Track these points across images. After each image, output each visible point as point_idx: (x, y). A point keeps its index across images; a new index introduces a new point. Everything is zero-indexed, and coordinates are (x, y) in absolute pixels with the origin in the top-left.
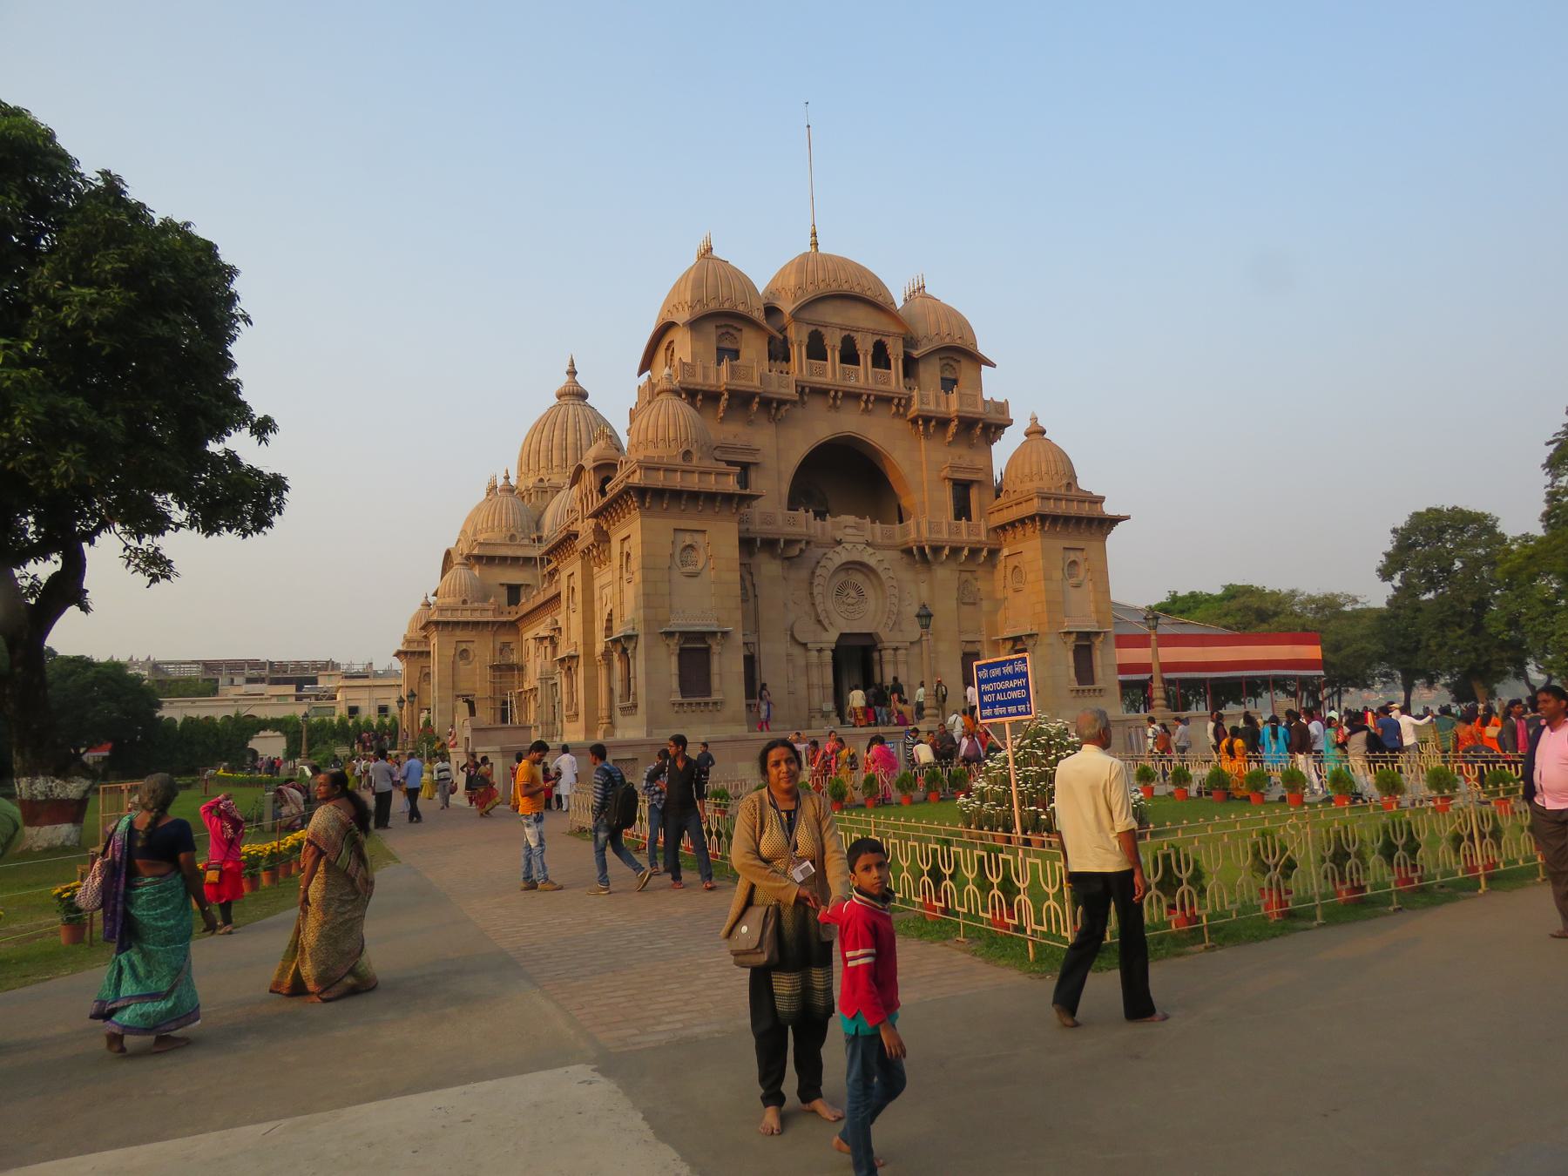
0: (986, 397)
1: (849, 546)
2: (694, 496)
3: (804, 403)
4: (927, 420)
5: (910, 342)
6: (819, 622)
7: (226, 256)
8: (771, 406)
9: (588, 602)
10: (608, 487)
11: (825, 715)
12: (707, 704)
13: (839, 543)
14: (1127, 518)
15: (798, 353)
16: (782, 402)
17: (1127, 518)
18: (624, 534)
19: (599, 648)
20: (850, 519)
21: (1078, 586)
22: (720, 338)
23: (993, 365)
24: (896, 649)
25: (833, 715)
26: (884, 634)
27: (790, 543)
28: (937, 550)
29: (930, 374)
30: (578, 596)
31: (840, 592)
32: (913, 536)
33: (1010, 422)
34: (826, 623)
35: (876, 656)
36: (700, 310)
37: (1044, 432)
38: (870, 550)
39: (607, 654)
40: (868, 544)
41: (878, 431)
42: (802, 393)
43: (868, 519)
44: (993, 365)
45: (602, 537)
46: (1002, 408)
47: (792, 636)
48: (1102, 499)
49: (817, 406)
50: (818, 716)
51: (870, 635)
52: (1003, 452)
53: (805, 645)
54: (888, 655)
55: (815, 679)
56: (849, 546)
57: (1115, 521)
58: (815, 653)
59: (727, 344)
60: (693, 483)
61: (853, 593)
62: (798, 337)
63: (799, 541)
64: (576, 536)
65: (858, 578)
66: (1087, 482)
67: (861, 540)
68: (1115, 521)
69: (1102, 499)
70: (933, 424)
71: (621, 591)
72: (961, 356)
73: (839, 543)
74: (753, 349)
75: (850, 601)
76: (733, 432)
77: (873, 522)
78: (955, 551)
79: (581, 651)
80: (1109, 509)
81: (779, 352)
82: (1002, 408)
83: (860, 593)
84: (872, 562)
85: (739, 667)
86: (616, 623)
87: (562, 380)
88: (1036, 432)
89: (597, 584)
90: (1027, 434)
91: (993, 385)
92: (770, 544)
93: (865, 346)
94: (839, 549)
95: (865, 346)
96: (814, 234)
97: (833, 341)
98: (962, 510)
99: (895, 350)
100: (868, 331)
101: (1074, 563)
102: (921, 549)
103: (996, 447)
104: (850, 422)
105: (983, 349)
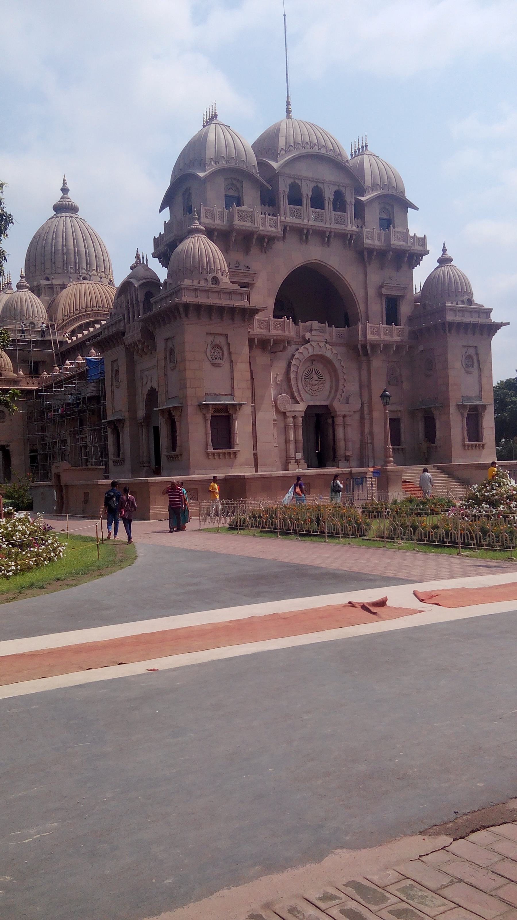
0: (411, 234)
2: (221, 310)
3: (284, 237)
4: (370, 251)
5: (360, 190)
6: (293, 398)
8: (265, 242)
9: (132, 381)
10: (152, 300)
11: (297, 461)
12: (229, 454)
13: (308, 341)
14: (508, 324)
15: (283, 200)
17: (508, 324)
18: (168, 335)
19: (141, 413)
20: (316, 324)
21: (469, 373)
22: (228, 187)
23: (417, 209)
24: (344, 417)
25: (302, 461)
28: (374, 346)
30: (123, 376)
31: (308, 376)
32: (360, 337)
33: (427, 252)
34: (298, 399)
35: (330, 421)
37: (450, 260)
39: (148, 418)
41: (335, 259)
42: (284, 230)
43: (327, 324)
44: (417, 209)
45: (149, 336)
46: (423, 241)
47: (276, 407)
48: (489, 311)
49: (292, 240)
50: (293, 461)
51: (326, 406)
52: (420, 275)
53: (285, 413)
54: (339, 421)
55: (292, 438)
56: (314, 344)
57: (497, 326)
58: (291, 419)
59: (232, 193)
61: (315, 377)
62: (284, 187)
63: (284, 341)
64: (123, 333)
65: (318, 366)
66: (480, 297)
67: (321, 339)
68: (497, 326)
69: (489, 311)
71: (166, 375)
72: (395, 203)
73: (308, 341)
74: (251, 198)
77: (330, 326)
78: (387, 346)
79: (126, 415)
80: (495, 318)
81: (269, 200)
82: (423, 241)
83: (320, 377)
85: (249, 428)
86: (162, 398)
87: (57, 196)
88: (444, 261)
89: (138, 368)
90: (439, 261)
91: (416, 225)
93: (329, 195)
94: (307, 346)
96: (288, 103)
98: (392, 317)
99: (350, 198)
101: (470, 357)
102: (364, 347)
103: (416, 271)
105: (409, 196)
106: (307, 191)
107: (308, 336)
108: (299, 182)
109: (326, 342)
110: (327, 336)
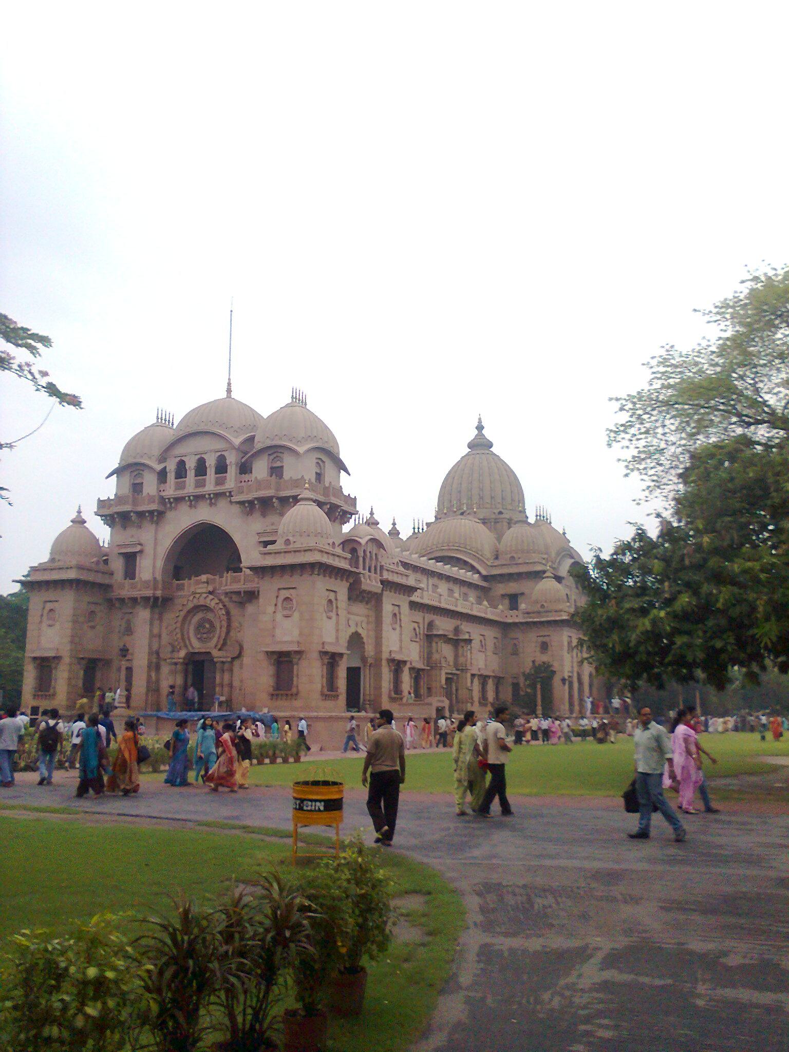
1: (197, 596)
4: (241, 503)
7: (265, 400)
15: (171, 477)
16: (151, 512)
24: (223, 662)
26: (215, 653)
27: (146, 599)
29: (260, 469)
31: (200, 626)
36: (124, 463)
38: (211, 597)
40: (210, 593)
41: (224, 517)
49: (184, 507)
60: (55, 576)
61: (207, 626)
65: (210, 616)
67: (204, 590)
70: (249, 507)
75: (205, 630)
76: (131, 536)
84: (213, 604)
92: (134, 600)
93: (211, 462)
95: (211, 462)
97: (191, 464)
99: (232, 459)
100: (211, 451)
104: (204, 514)
106: (191, 464)
107: (192, 589)
108: (183, 458)
109: (210, 593)
110: (210, 588)
